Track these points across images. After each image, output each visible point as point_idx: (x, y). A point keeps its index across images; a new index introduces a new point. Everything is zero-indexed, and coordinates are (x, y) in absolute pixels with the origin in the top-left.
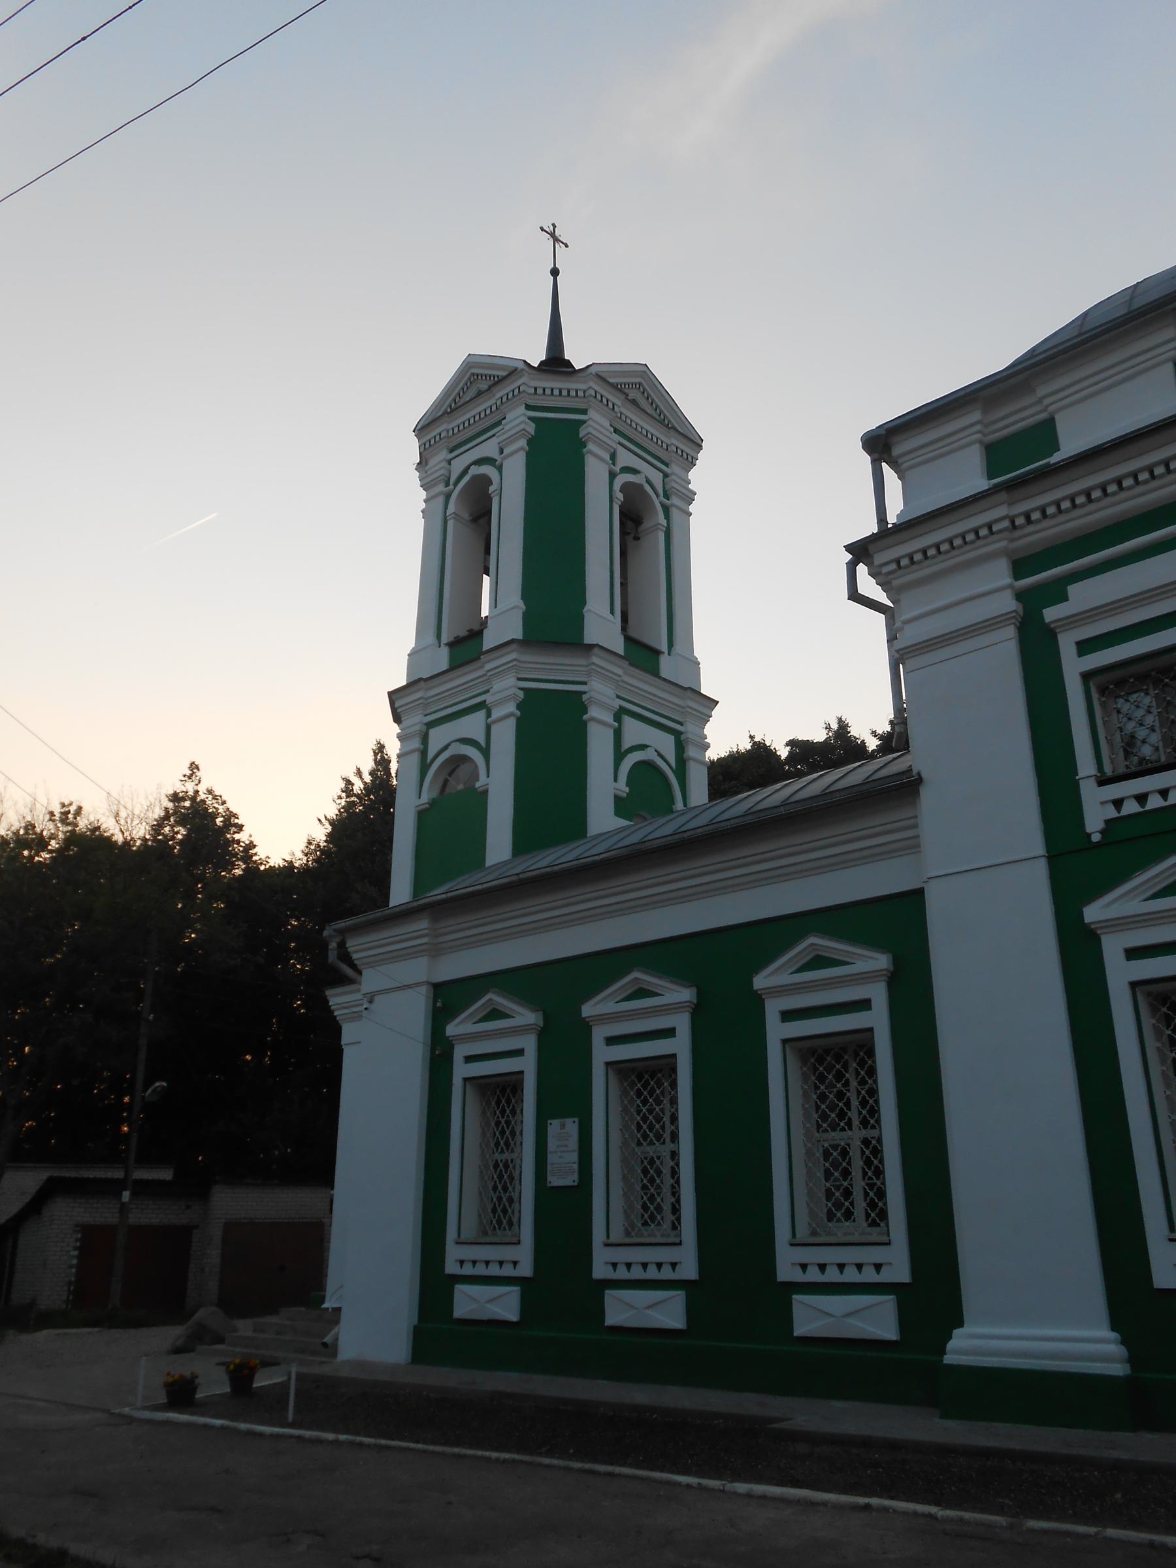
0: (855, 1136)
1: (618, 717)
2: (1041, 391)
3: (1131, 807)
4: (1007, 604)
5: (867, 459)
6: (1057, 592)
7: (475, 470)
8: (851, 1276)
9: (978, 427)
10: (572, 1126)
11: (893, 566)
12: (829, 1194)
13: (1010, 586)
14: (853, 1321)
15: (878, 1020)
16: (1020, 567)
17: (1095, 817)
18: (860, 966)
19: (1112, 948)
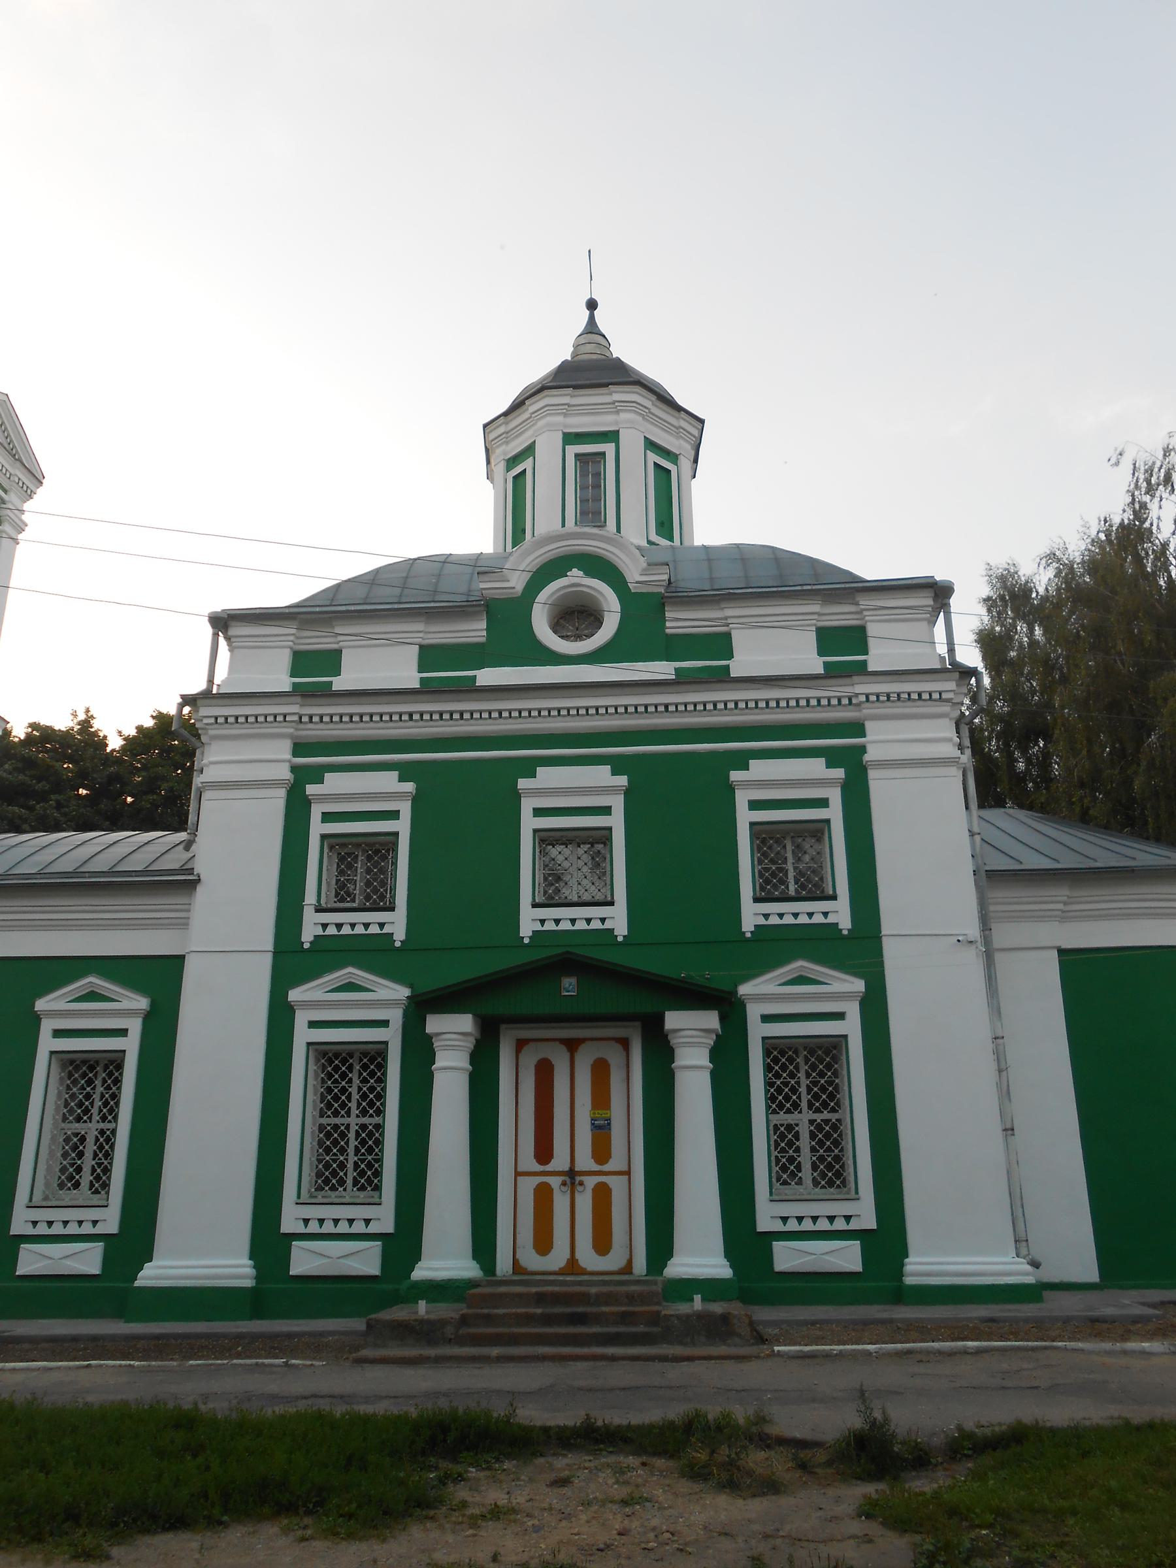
0: (91, 1129)
2: (338, 630)
3: (331, 930)
4: (285, 773)
5: (209, 630)
6: (317, 774)
8: (73, 1229)
9: (292, 638)
11: (212, 720)
12: (63, 1170)
13: (289, 761)
14: (68, 1262)
15: (131, 1046)
16: (299, 748)
17: (309, 933)
18: (125, 1004)
19: (301, 1019)
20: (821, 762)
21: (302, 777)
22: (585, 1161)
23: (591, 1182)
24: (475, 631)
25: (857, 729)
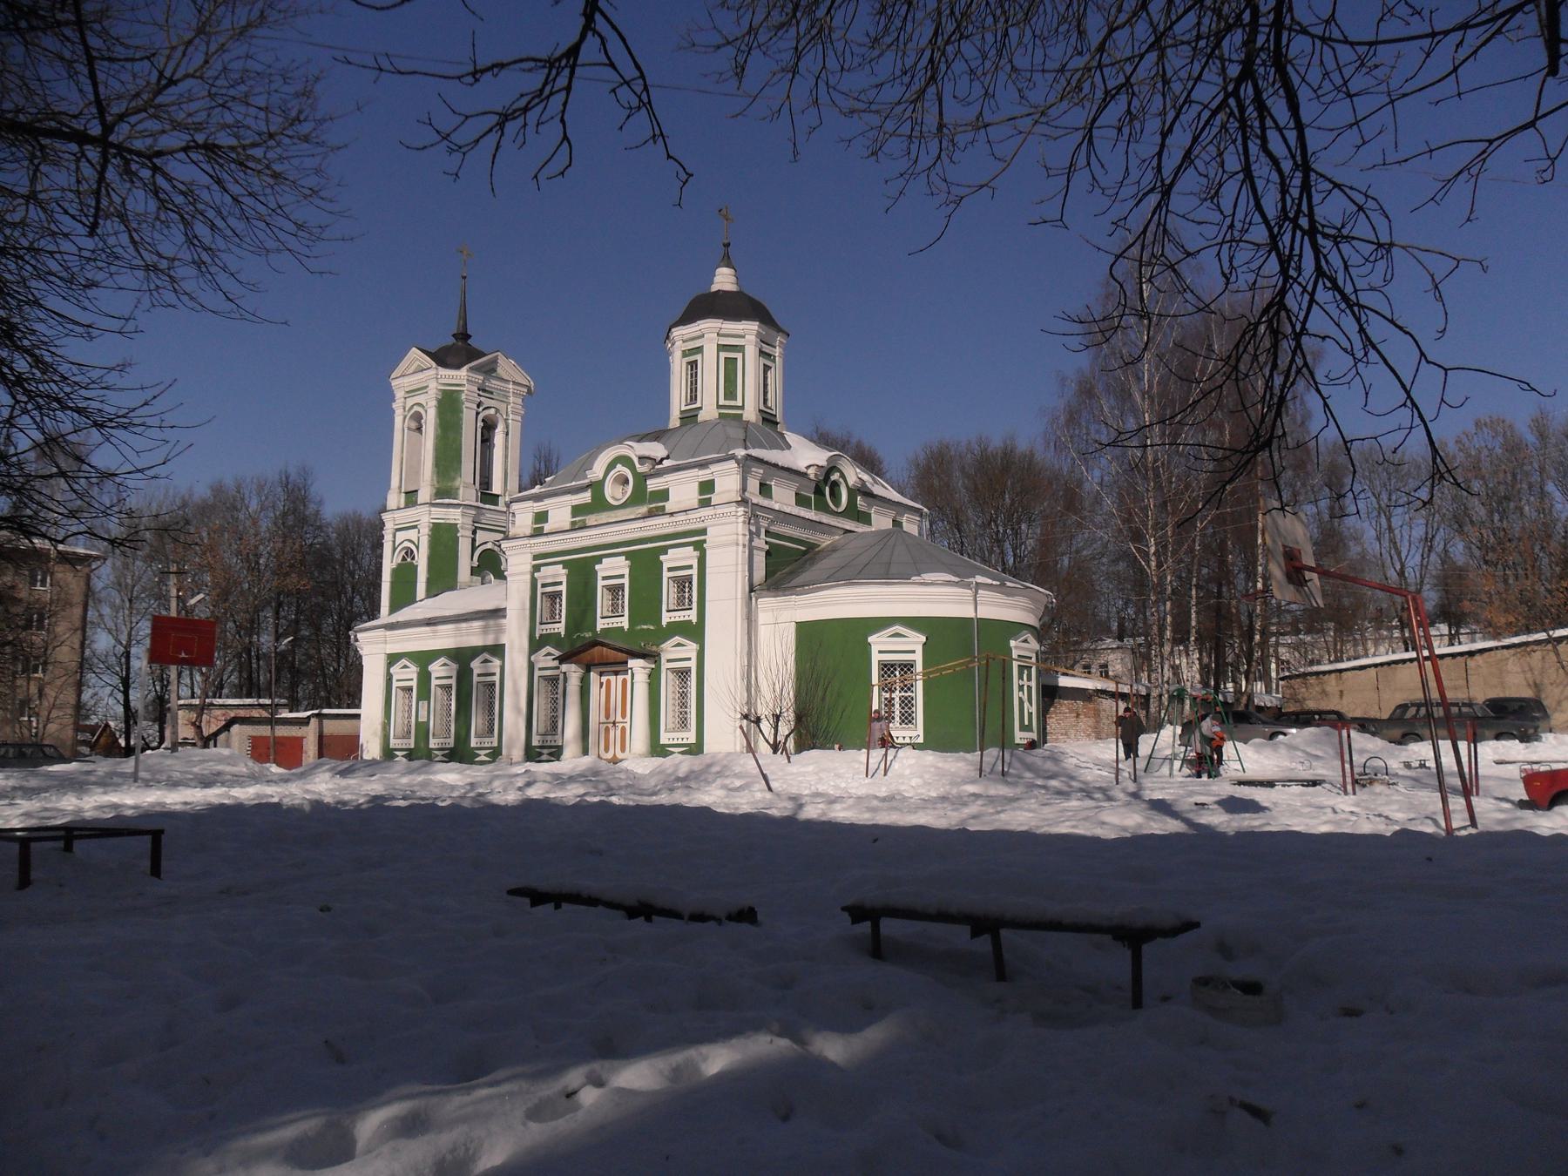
1: (474, 532)
4: (528, 568)
7: (416, 408)
10: (426, 702)
16: (536, 557)
20: (691, 548)
21: (536, 568)
22: (619, 718)
23: (620, 726)
24: (586, 497)
25: (703, 532)
